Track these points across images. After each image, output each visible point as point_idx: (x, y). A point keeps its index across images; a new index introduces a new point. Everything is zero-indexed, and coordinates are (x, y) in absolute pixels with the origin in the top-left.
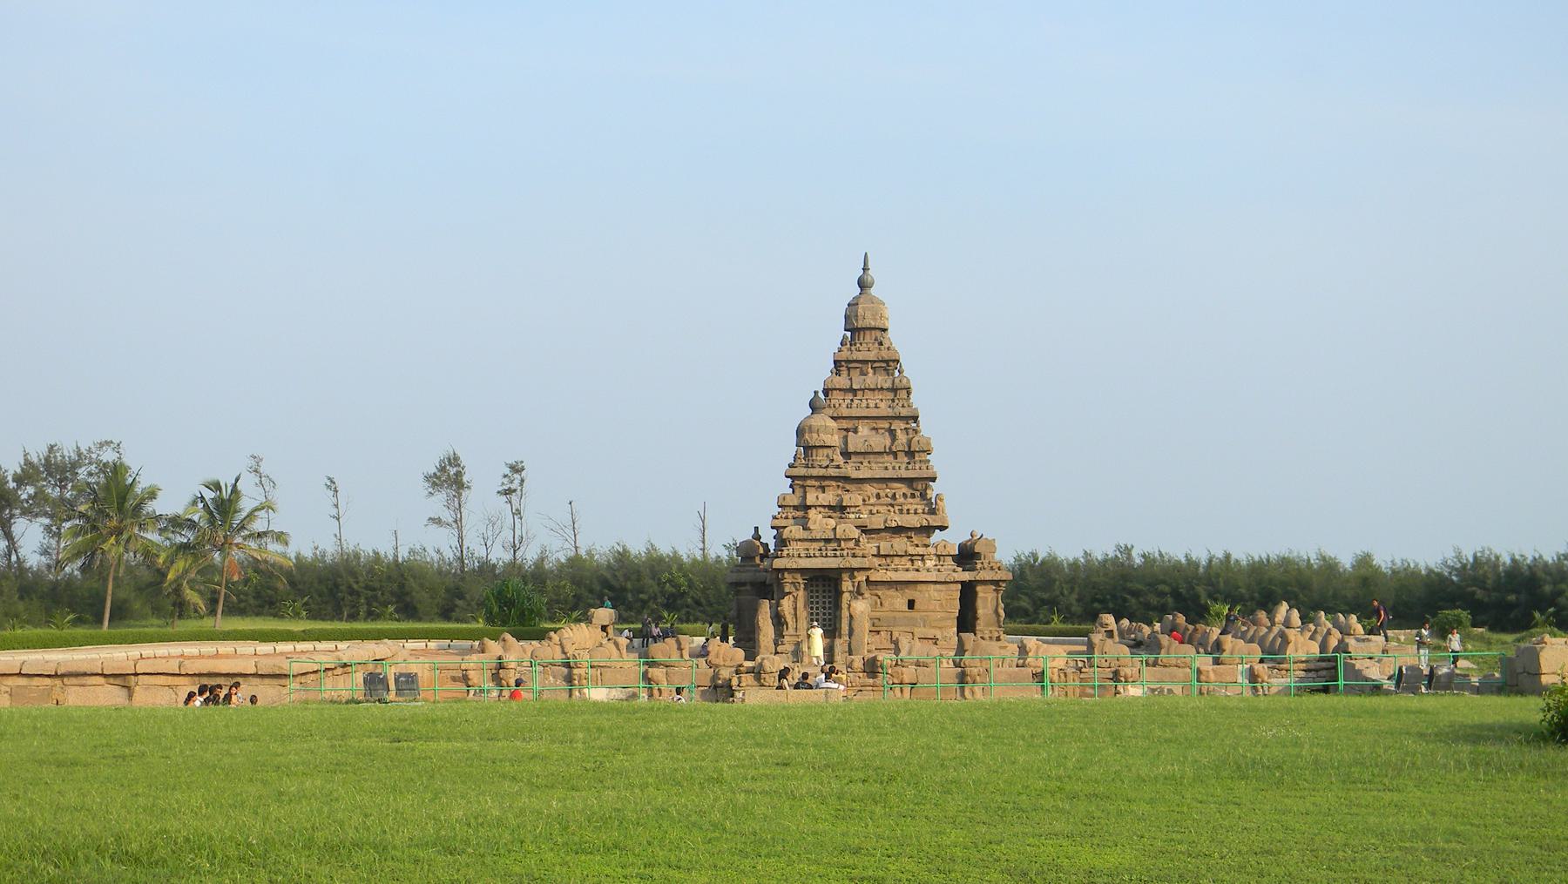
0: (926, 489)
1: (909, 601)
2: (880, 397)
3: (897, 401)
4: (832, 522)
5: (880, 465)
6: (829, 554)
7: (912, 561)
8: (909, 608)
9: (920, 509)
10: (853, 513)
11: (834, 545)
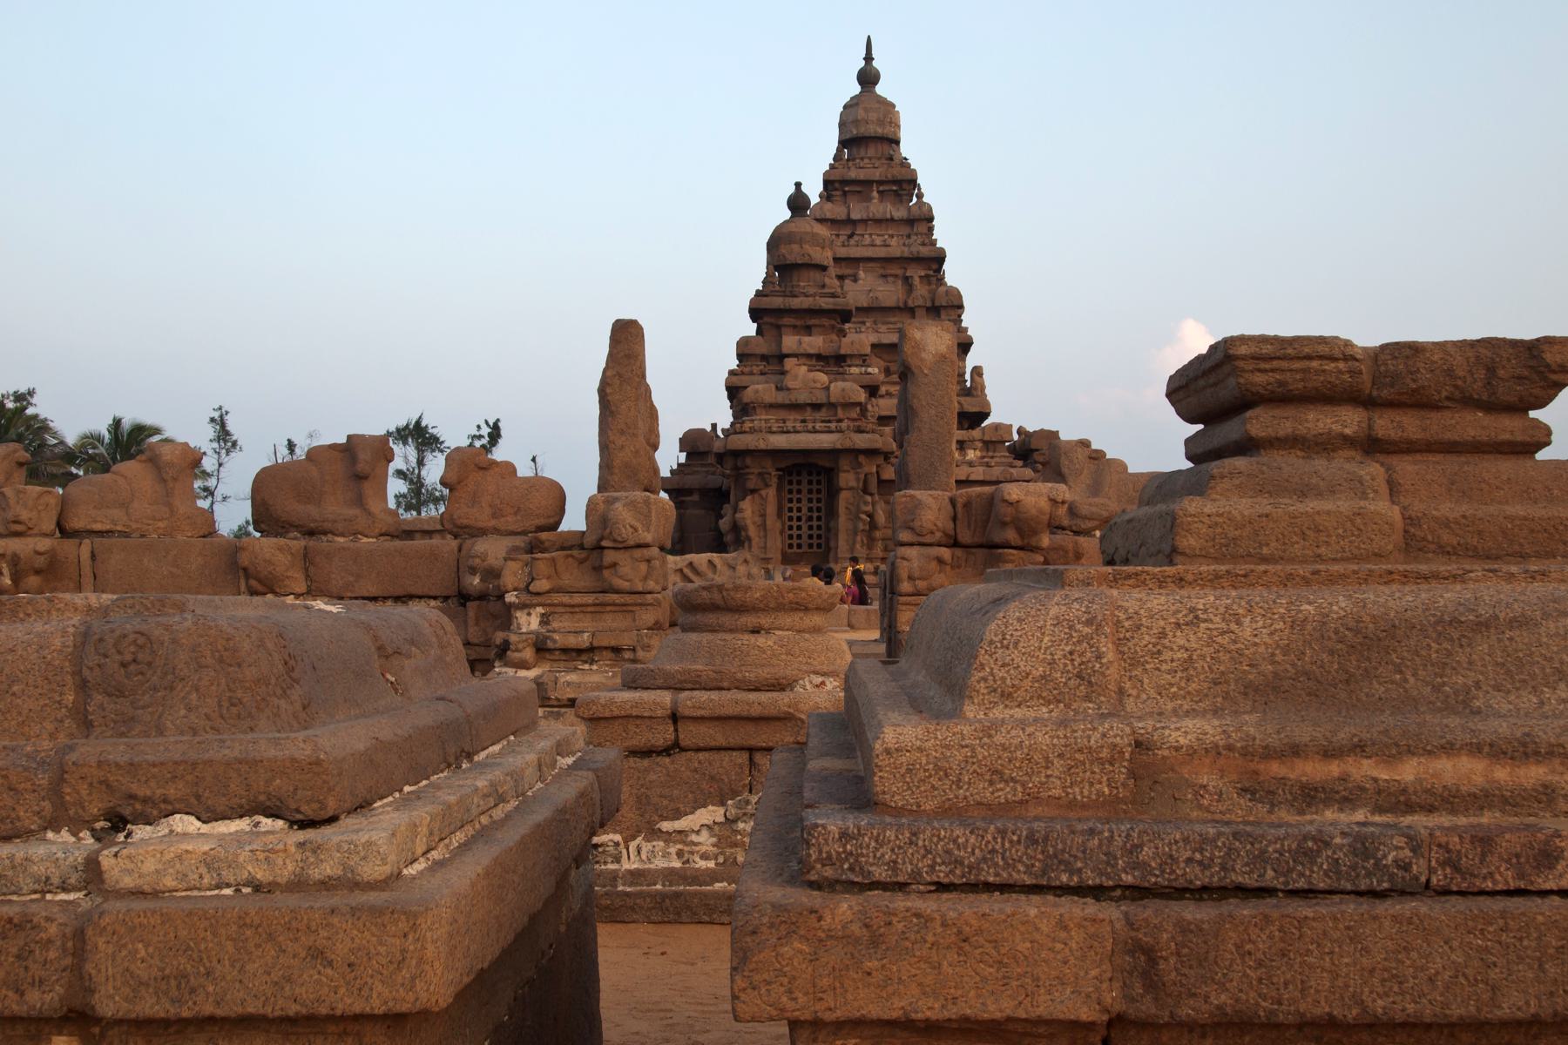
2: (890, 232)
4: (823, 378)
5: (891, 326)
6: (817, 428)
10: (857, 366)
11: (823, 414)
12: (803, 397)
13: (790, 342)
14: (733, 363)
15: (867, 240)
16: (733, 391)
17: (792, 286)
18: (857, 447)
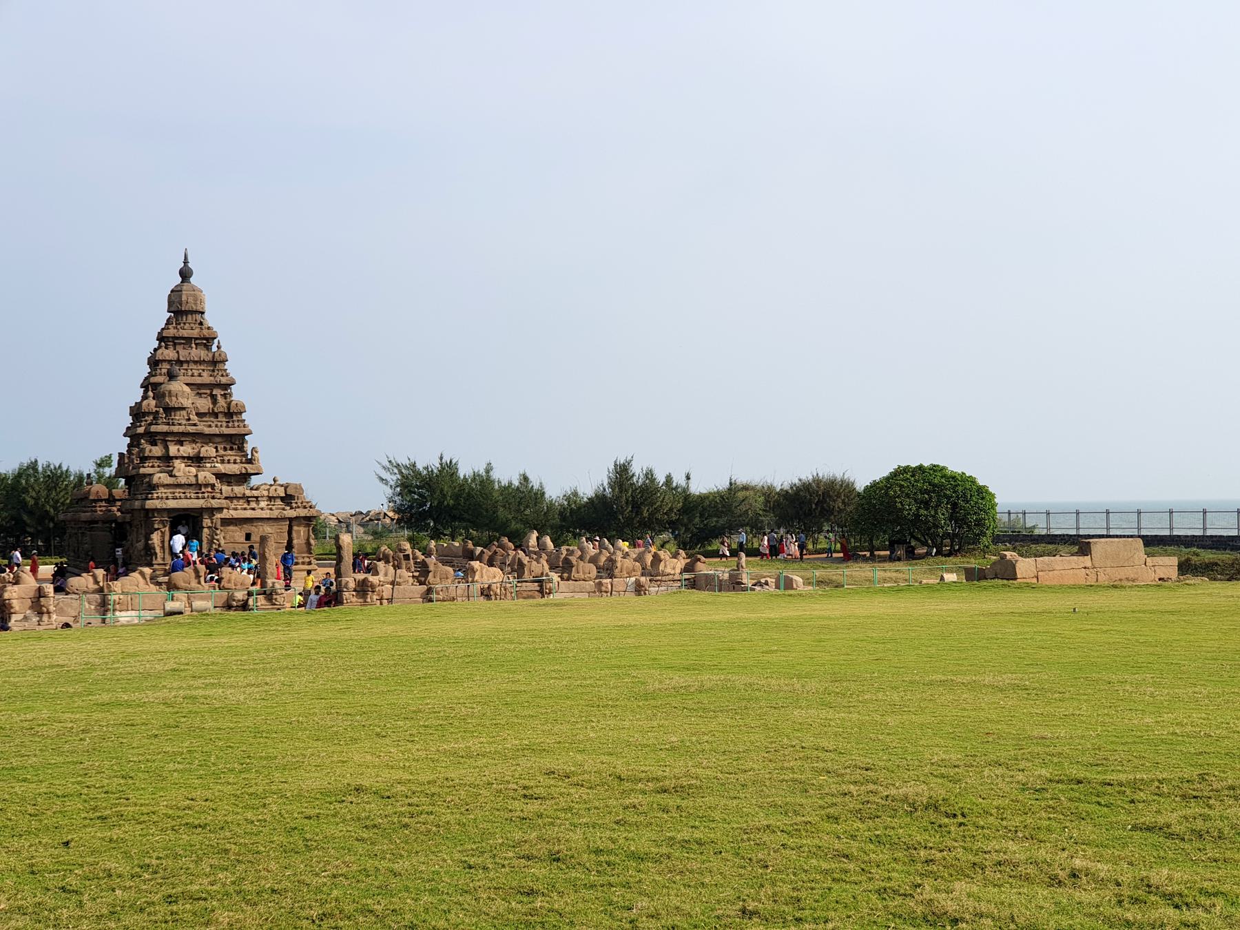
0: (243, 443)
1: (246, 534)
2: (202, 368)
3: (216, 372)
4: (193, 470)
6: (192, 497)
7: (248, 502)
8: (246, 540)
9: (238, 460)
10: (209, 463)
12: (183, 481)
13: (173, 450)
15: (190, 373)
17: (172, 419)
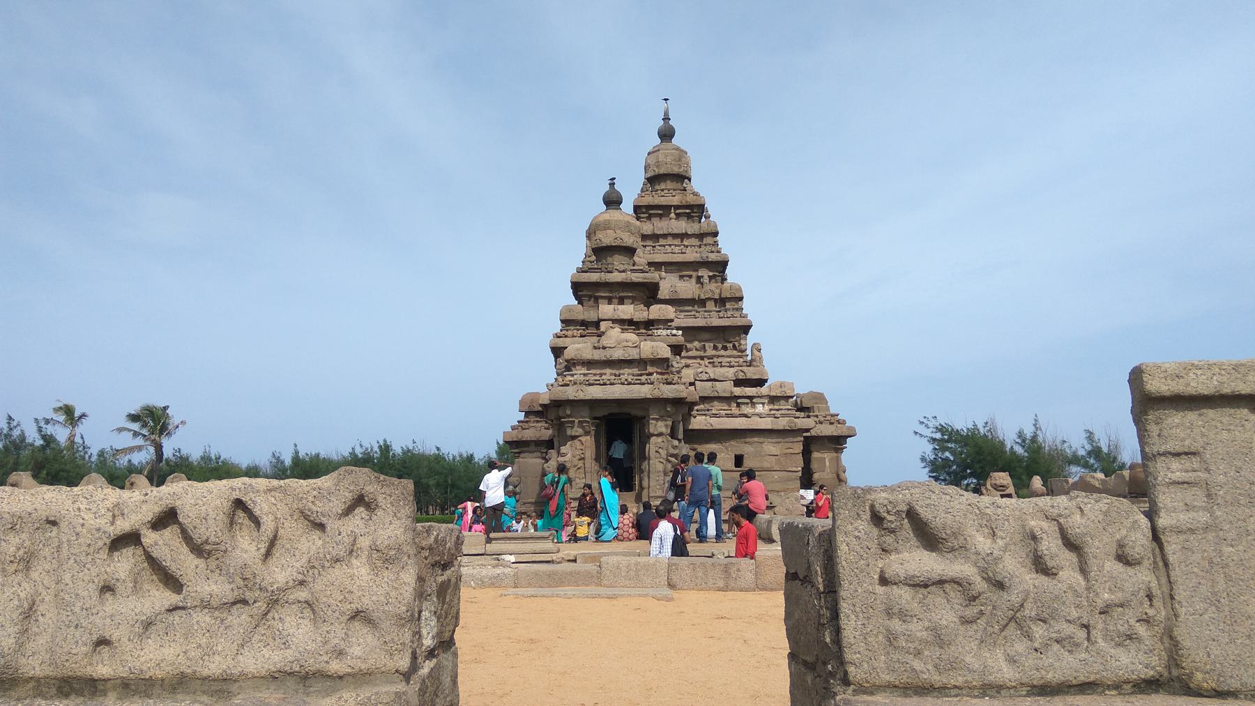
0: (739, 341)
1: (736, 456)
2: (686, 244)
7: (738, 405)
12: (618, 354)
13: (606, 310)
14: (558, 327)
16: (557, 351)
18: (665, 396)
